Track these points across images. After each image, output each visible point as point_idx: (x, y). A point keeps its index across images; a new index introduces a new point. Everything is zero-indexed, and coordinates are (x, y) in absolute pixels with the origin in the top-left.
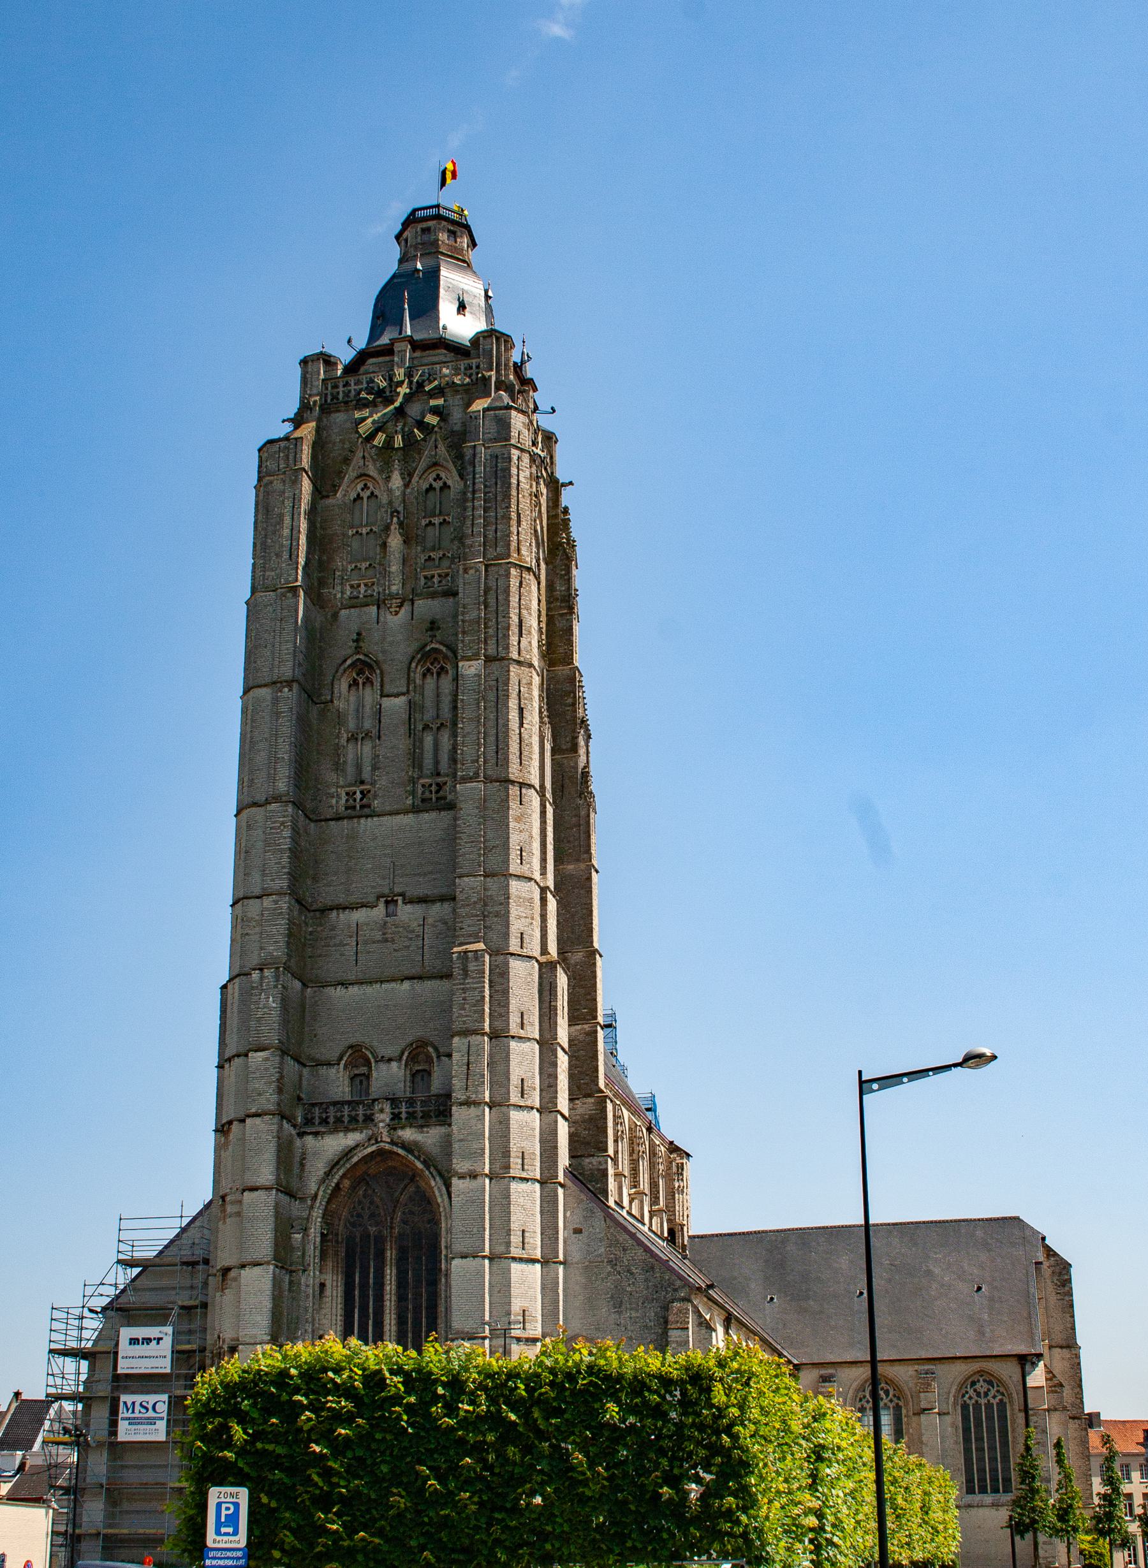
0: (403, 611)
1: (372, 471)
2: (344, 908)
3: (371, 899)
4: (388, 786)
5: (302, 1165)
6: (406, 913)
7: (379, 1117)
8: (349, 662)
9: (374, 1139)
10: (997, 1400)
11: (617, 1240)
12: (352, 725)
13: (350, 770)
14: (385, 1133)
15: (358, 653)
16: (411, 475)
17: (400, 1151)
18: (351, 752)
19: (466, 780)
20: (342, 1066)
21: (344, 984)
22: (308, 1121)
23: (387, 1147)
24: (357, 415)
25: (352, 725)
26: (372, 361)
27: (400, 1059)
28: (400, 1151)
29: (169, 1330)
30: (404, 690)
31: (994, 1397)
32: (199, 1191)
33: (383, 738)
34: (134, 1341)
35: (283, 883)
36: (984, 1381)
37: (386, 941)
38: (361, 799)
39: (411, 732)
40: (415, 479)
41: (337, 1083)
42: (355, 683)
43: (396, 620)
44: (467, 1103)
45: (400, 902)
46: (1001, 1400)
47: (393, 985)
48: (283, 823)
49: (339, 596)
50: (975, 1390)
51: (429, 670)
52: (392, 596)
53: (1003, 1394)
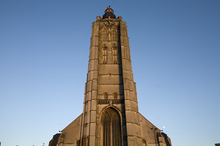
0: (110, 42)
3: (108, 74)
6: (112, 76)
18: (103, 57)
21: (104, 84)
23: (112, 107)
27: (112, 95)
32: (81, 111)
42: (104, 50)
43: (110, 43)
44: (127, 99)
47: (111, 85)
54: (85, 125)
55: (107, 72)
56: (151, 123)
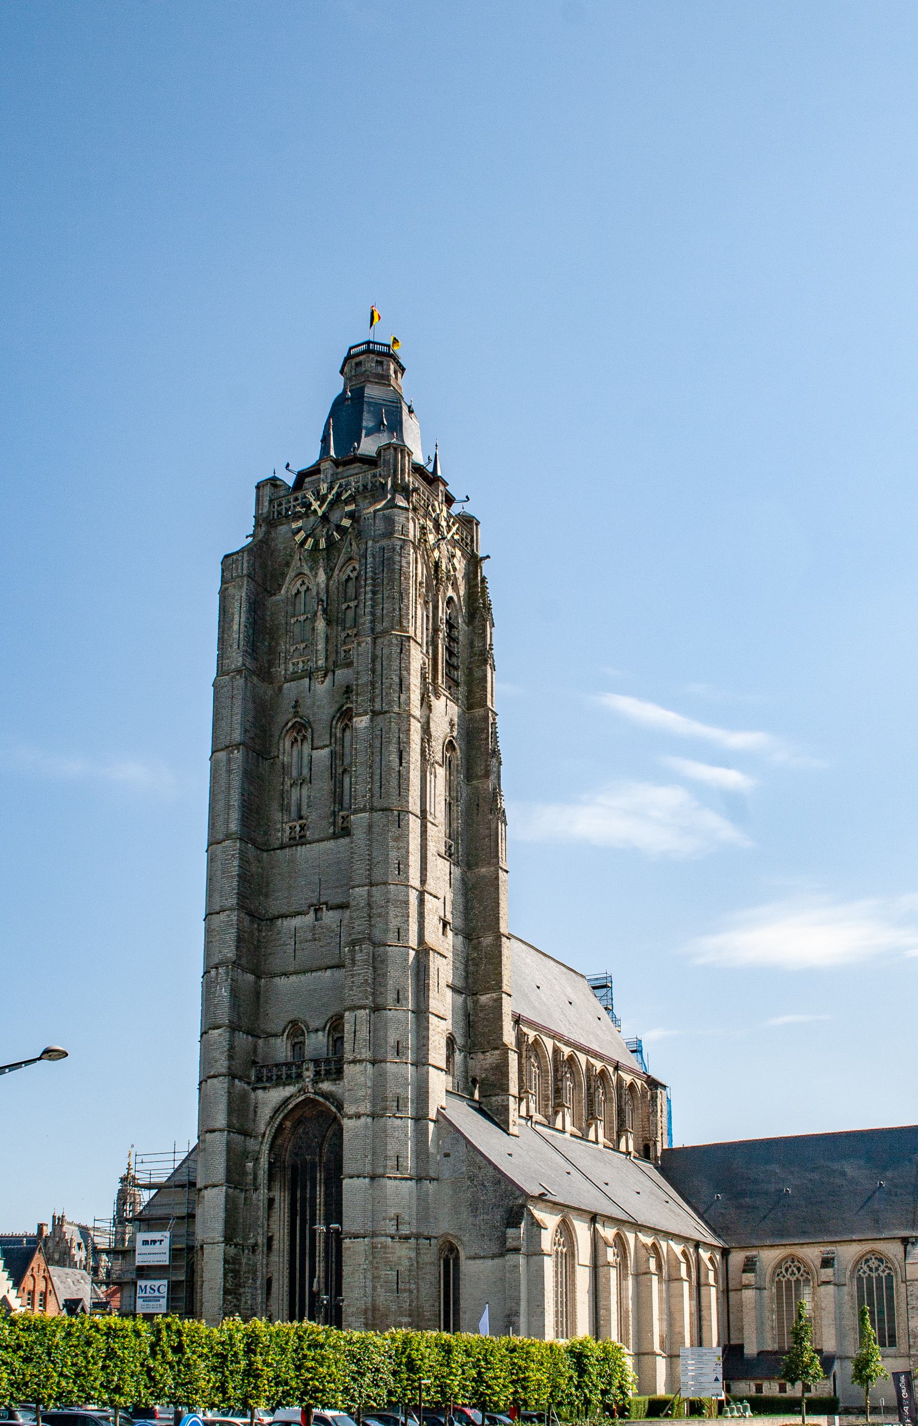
0: (327, 679)
1: (306, 570)
2: (286, 917)
3: (305, 908)
4: (317, 819)
5: (255, 1112)
7: (306, 1074)
8: (290, 724)
9: (302, 1090)
10: (885, 1274)
11: (475, 1161)
12: (294, 773)
13: (294, 809)
14: (310, 1087)
15: (295, 717)
16: (332, 570)
17: (321, 1099)
18: (295, 794)
19: (356, 812)
20: (285, 1036)
21: (286, 974)
22: (259, 1079)
23: (312, 1096)
24: (294, 526)
25: (294, 773)
26: (307, 480)
28: (321, 1099)
29: (167, 1234)
30: (328, 743)
31: (883, 1271)
33: (313, 781)
34: (145, 1242)
35: (233, 901)
36: (876, 1258)
37: (315, 940)
39: (333, 776)
40: (336, 572)
41: (281, 1049)
43: (322, 688)
44: (354, 1062)
45: (324, 909)
46: (889, 1274)
47: (319, 973)
48: (233, 855)
49: (283, 672)
50: (868, 1266)
52: (318, 669)
53: (890, 1269)
54: (626, 1097)
55: (303, 896)
56: (490, 1162)
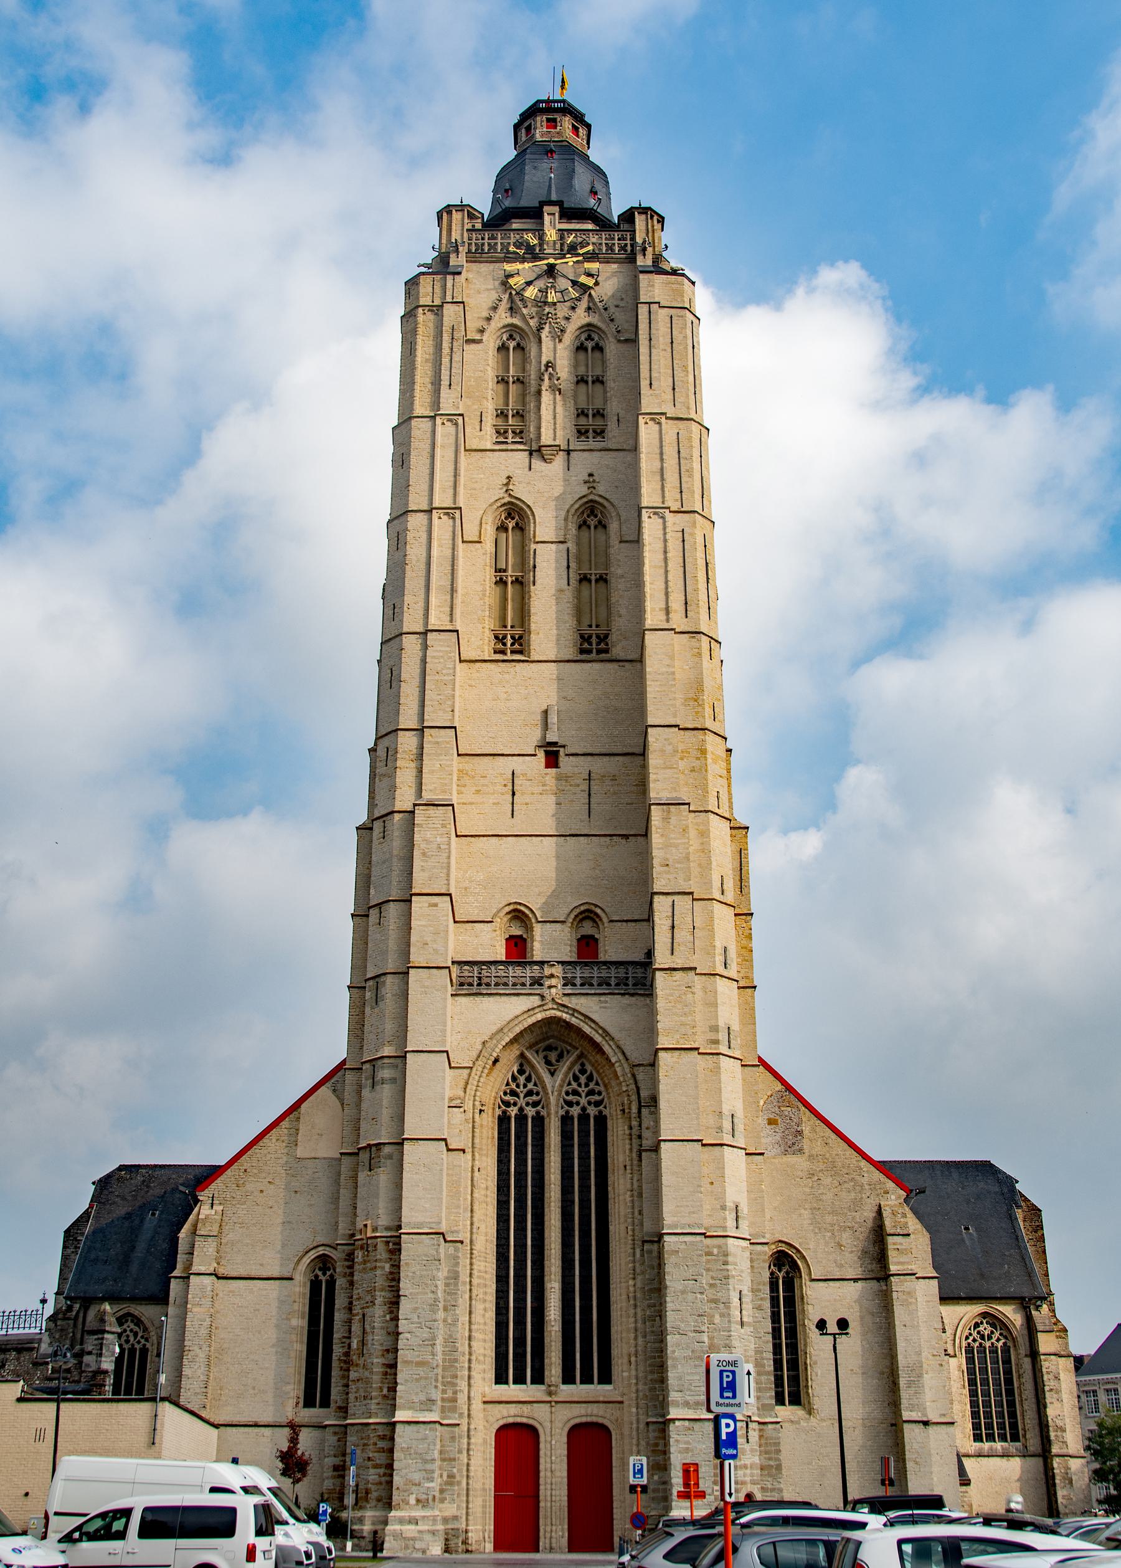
31: (998, 1340)
38: (512, 644)
50: (979, 1332)
51: (585, 522)
